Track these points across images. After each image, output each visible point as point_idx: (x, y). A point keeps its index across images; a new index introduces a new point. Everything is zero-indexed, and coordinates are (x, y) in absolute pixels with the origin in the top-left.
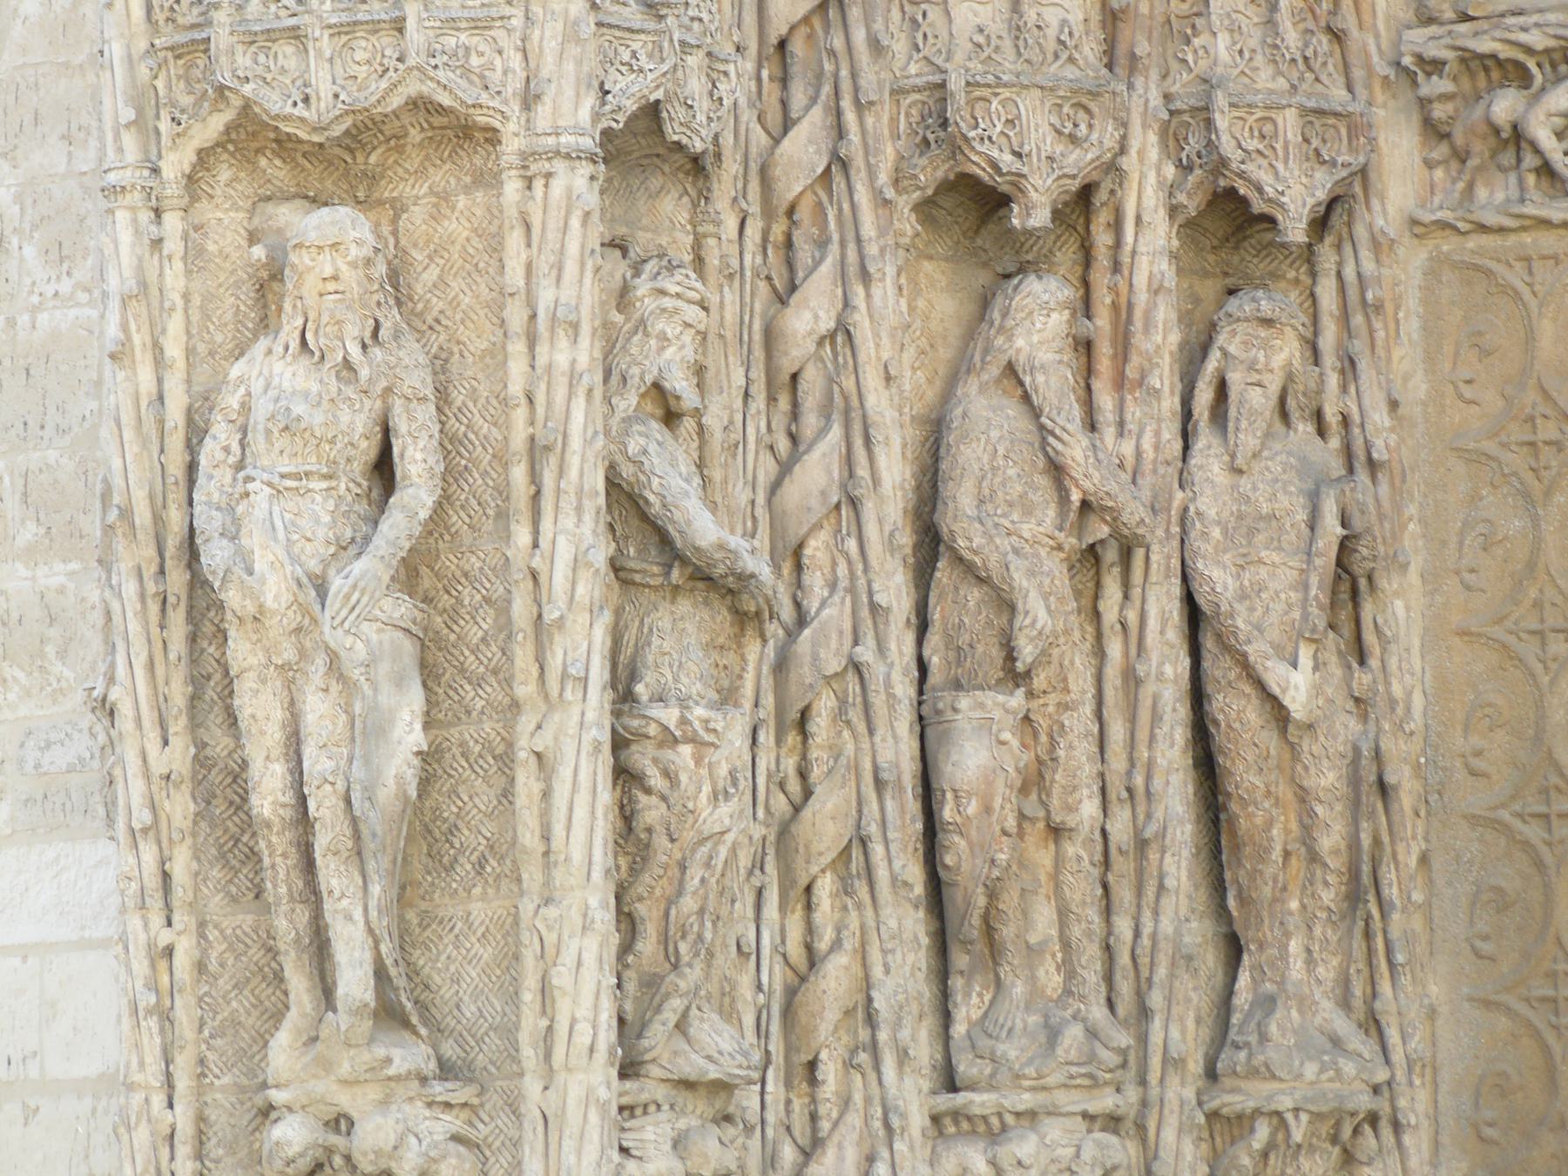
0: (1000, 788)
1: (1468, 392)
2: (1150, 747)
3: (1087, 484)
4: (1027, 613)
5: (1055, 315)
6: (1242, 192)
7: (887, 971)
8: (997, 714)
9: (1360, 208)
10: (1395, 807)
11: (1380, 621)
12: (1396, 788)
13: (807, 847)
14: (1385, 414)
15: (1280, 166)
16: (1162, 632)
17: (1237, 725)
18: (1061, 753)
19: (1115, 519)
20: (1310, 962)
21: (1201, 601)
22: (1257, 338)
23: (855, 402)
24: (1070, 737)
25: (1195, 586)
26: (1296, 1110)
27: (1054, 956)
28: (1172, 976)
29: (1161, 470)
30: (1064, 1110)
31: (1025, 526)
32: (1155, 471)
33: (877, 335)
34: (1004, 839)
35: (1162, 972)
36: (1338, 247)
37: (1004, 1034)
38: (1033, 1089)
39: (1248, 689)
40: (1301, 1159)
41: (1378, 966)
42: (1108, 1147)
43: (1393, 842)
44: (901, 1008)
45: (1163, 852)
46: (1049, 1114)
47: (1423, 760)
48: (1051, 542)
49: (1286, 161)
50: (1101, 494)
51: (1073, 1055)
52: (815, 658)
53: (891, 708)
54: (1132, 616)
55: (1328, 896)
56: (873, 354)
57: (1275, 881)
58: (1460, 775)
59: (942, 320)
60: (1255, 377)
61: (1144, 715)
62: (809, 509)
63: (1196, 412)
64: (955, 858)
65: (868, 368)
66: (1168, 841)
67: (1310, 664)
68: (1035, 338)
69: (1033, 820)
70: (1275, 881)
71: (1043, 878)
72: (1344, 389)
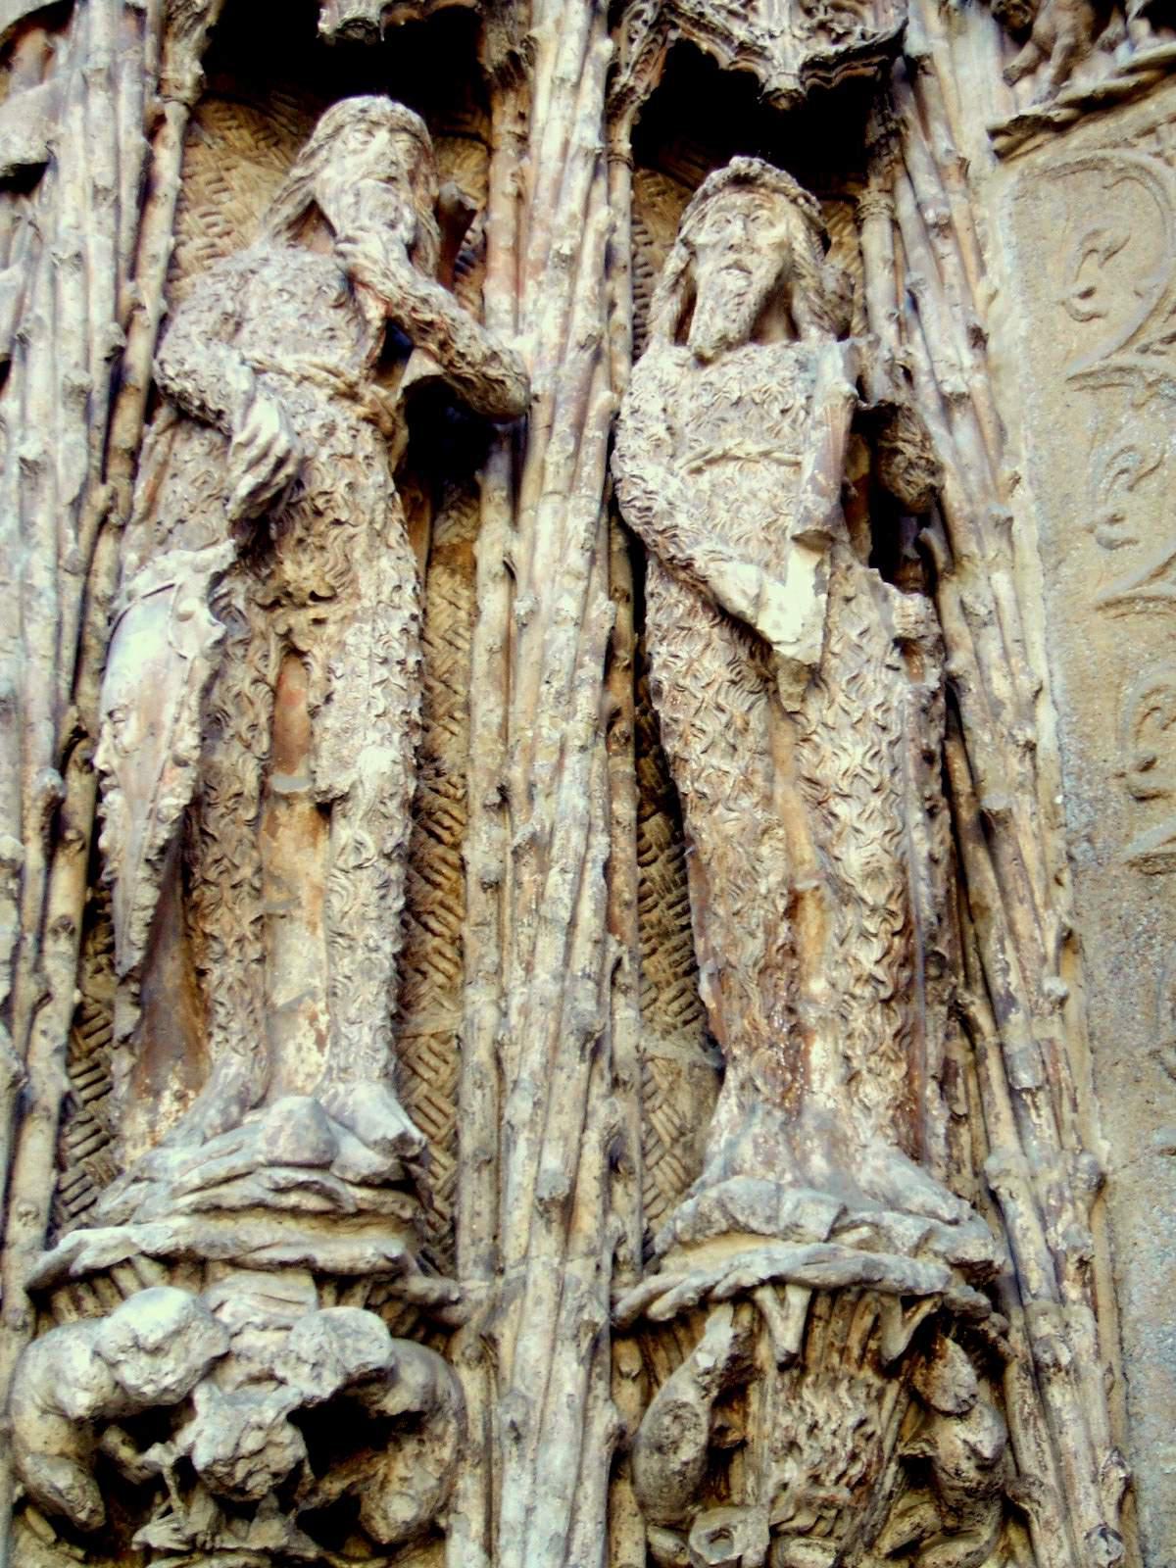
1: (1086, 306)
5: (382, 136)
6: (705, 46)
9: (914, 135)
10: (1006, 851)
11: (969, 599)
12: (1004, 819)
17: (687, 682)
19: (443, 345)
20: (851, 1078)
26: (778, 1282)
28: (550, 1066)
29: (571, 355)
30: (265, 1256)
32: (561, 359)
33: (90, 151)
36: (890, 192)
38: (197, 1211)
39: (703, 624)
40: (807, 1394)
41: (992, 1104)
42: (357, 1333)
45: (544, 869)
46: (234, 1264)
47: (1059, 799)
48: (333, 379)
49: (770, 16)
50: (411, 302)
51: (284, 1150)
54: (519, 549)
55: (868, 956)
58: (1120, 801)
60: (731, 257)
65: (69, 187)
66: (555, 851)
69: (288, 799)
70: (770, 931)
71: (305, 894)
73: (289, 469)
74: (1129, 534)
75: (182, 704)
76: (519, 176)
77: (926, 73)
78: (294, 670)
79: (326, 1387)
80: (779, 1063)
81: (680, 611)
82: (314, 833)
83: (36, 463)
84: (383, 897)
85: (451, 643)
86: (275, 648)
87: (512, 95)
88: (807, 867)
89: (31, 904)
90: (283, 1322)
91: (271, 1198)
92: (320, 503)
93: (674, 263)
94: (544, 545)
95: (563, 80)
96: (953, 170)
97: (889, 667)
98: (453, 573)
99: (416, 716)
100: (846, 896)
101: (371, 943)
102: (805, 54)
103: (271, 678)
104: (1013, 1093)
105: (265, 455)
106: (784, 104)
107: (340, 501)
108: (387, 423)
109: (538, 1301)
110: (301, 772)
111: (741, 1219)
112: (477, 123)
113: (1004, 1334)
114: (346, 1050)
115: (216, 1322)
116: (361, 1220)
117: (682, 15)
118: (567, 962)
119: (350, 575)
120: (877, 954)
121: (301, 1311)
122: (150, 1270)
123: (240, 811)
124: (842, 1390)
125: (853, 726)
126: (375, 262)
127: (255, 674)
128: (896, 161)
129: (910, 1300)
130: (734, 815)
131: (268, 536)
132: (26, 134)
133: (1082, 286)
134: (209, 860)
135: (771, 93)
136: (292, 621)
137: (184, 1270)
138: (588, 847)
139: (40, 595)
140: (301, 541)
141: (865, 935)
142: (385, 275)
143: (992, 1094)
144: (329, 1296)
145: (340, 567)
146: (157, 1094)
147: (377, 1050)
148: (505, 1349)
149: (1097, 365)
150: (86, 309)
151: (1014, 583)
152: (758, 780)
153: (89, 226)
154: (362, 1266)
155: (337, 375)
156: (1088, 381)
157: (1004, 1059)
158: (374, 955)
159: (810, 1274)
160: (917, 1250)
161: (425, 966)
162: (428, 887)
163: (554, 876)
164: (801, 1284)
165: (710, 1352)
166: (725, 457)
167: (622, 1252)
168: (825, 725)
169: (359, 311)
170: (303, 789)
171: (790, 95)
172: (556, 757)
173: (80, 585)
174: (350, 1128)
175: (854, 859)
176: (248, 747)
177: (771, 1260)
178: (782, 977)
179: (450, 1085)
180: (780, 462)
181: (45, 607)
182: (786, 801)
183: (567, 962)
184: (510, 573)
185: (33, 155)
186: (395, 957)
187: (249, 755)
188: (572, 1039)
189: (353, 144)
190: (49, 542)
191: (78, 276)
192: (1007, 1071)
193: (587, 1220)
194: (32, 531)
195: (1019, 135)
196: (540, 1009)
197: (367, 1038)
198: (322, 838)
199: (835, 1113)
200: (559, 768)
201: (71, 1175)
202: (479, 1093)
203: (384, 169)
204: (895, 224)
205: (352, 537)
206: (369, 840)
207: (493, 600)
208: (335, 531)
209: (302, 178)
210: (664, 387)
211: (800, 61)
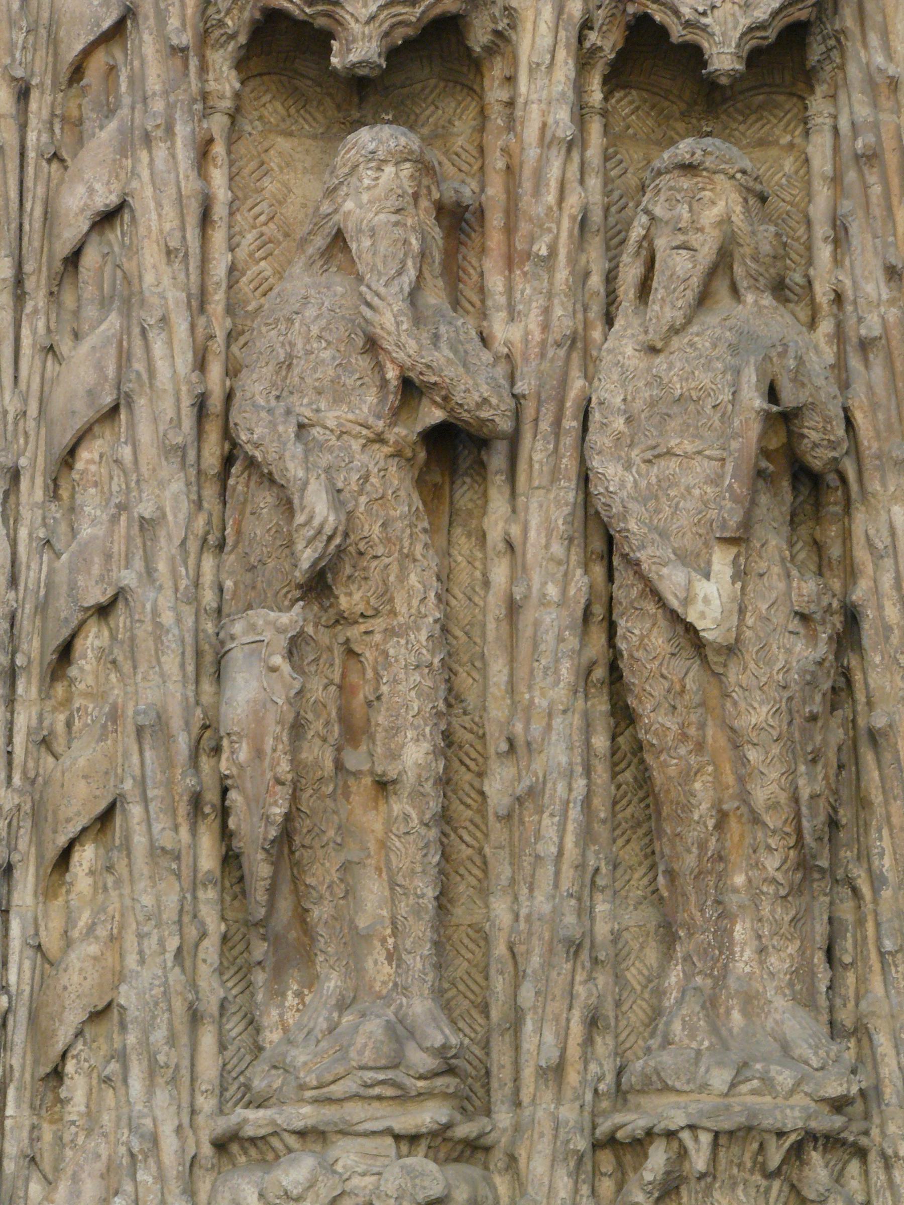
2: (530, 688)
3: (400, 356)
4: (303, 509)
5: (389, 169)
6: (658, 18)
7: (142, 962)
8: (267, 636)
9: (853, 46)
10: (888, 756)
11: (872, 532)
13: (55, 813)
14: (882, 285)
17: (640, 654)
18: (385, 689)
19: (446, 399)
20: (762, 951)
22: (679, 191)
24: (394, 669)
27: (384, 941)
29: (550, 354)
30: (361, 1128)
31: (331, 414)
32: (543, 355)
33: (159, 205)
34: (278, 788)
35: (536, 960)
37: (301, 1037)
38: (316, 1101)
40: (717, 1194)
43: (886, 803)
44: (156, 1004)
45: (540, 811)
46: (343, 1133)
48: (365, 432)
51: (368, 1057)
52: (73, 586)
53: (158, 640)
54: (515, 531)
55: (772, 863)
56: (154, 225)
57: (702, 846)
59: (304, 206)
60: (681, 238)
61: (524, 647)
62: (73, 413)
63: (621, 292)
67: (729, 571)
68: (365, 197)
69: (357, 774)
70: (702, 846)
71: (372, 846)
72: (837, 261)
73: (337, 541)
75: (277, 739)
78: (352, 663)
80: (709, 944)
81: (634, 593)
82: (376, 800)
83: (152, 519)
84: (425, 855)
85: (470, 599)
86: (338, 651)
87: (499, 59)
88: (731, 791)
89: (186, 872)
90: (375, 1170)
91: (362, 1091)
92: (362, 546)
93: (636, 232)
94: (532, 534)
95: (538, 64)
96: (884, 90)
97: (791, 632)
98: (469, 536)
99: (442, 706)
100: (756, 820)
103: (337, 680)
104: (882, 954)
105: (319, 532)
106: (724, 81)
107: (377, 540)
108: (408, 453)
109: (542, 1135)
110: (363, 748)
111: (670, 1083)
112: (471, 76)
113: (866, 1133)
114: (407, 972)
115: (334, 1172)
116: (422, 1098)
118: (556, 886)
119: (389, 594)
120: (777, 864)
121: (386, 1161)
122: (292, 1141)
123: (324, 788)
124: (740, 1192)
125: (760, 689)
126: (389, 334)
127: (326, 681)
128: (837, 67)
130: (675, 761)
131: (326, 582)
132: (106, 178)
134: (305, 831)
135: (710, 73)
136: (349, 634)
137: (310, 1138)
138: (570, 790)
139: (168, 632)
140: (349, 577)
142: (399, 346)
143: (868, 950)
144: (404, 1148)
146: (283, 995)
147: (426, 974)
150: (173, 365)
152: (692, 731)
153: (166, 281)
154: (424, 1130)
155: (368, 427)
157: (878, 925)
158: (421, 901)
160: (792, 1092)
161: (462, 871)
162: (462, 807)
163: (546, 821)
165: (652, 1170)
167: (602, 1087)
168: (741, 687)
169: (379, 367)
170: (366, 767)
171: (727, 73)
172: (546, 719)
173: (194, 610)
174: (412, 1034)
175: (760, 795)
176: (325, 740)
177: (688, 1115)
178: (711, 881)
179: (483, 964)
180: (710, 458)
181: (171, 641)
182: (715, 741)
183: (556, 886)
185: (113, 199)
186: (437, 898)
187: (326, 746)
188: (560, 945)
189: (367, 182)
190: (168, 584)
191: (163, 335)
192: (879, 939)
193: (573, 1077)
194: (156, 575)
196: (538, 923)
197: (419, 965)
198: (381, 802)
199: (751, 975)
200: (549, 727)
201: (232, 1049)
202: (500, 978)
204: (836, 131)
205: (387, 566)
206: (414, 816)
207: (500, 573)
208: (374, 564)
209: (329, 214)
211: (741, 29)
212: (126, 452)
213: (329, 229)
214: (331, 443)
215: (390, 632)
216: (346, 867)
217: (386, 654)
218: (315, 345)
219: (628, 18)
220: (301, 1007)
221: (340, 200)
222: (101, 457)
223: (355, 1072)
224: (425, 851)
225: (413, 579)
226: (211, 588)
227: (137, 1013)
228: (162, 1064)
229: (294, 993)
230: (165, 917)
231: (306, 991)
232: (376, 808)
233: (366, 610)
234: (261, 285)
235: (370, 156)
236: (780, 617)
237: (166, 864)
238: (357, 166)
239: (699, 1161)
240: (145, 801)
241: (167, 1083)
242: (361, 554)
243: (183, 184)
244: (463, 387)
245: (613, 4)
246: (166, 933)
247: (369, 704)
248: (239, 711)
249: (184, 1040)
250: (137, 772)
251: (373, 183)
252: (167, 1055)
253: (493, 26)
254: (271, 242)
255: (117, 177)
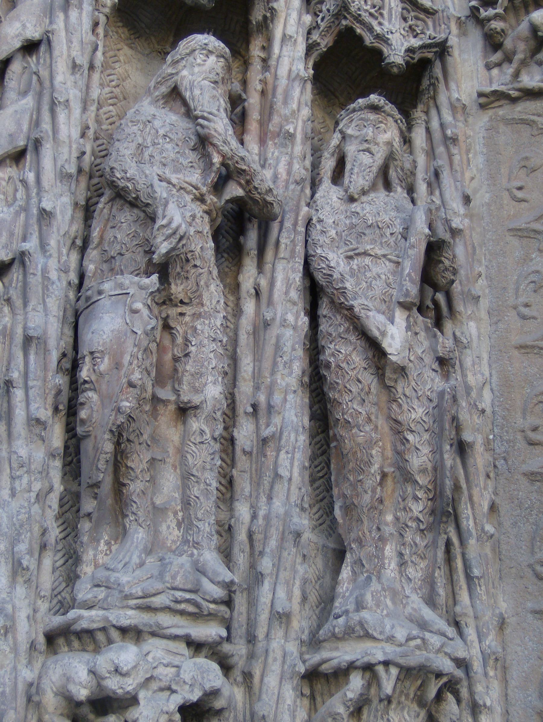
0: (130, 348)
1: (520, 194)
2: (273, 373)
3: (225, 149)
6: (359, 31)
7: (13, 494)
8: (131, 291)
9: (442, 86)
10: (470, 461)
11: (458, 334)
12: (471, 445)
15: (386, 23)
16: (287, 293)
17: (344, 365)
18: (193, 349)
20: (402, 564)
21: (319, 277)
22: (367, 120)
23: (47, 84)
25: (315, 264)
26: (386, 664)
28: (281, 547)
29: (292, 187)
32: (287, 187)
35: (273, 543)
36: (427, 113)
37: (120, 566)
38: (139, 608)
39: (353, 338)
40: (391, 713)
44: (21, 526)
45: (278, 450)
46: (154, 634)
47: (491, 437)
48: (194, 191)
49: (390, 21)
50: (236, 158)
51: (179, 582)
53: (45, 288)
54: (263, 283)
55: (417, 508)
56: (65, 53)
58: (521, 444)
60: (366, 146)
61: (269, 350)
64: (89, 412)
65: (59, 59)
66: (283, 442)
67: (404, 324)
69: (165, 402)
70: (374, 491)
71: (171, 450)
74: (535, 314)
76: (264, 82)
77: (449, 55)
79: (195, 696)
80: (373, 554)
81: (342, 329)
84: (213, 459)
88: (389, 461)
91: (172, 605)
96: (459, 110)
97: (433, 370)
101: (208, 482)
102: (406, 45)
104: (469, 578)
105: (174, 233)
106: (395, 70)
109: (275, 660)
111: (370, 631)
117: (349, 13)
118: (288, 498)
119: (198, 293)
120: (421, 508)
122: (115, 634)
125: (418, 398)
126: (220, 134)
128: (431, 98)
129: (439, 675)
130: (363, 434)
132: (34, 23)
133: (519, 184)
134: (131, 430)
135: (389, 63)
136: (169, 312)
137: (132, 634)
138: (296, 441)
139: (53, 283)
140: (179, 273)
141: (416, 499)
142: (225, 143)
143: (458, 576)
145: (194, 288)
146: (98, 541)
147: (212, 535)
148: (256, 679)
149: (524, 226)
151: (478, 328)
152: (373, 418)
153: (69, 84)
155: (197, 188)
156: (517, 232)
158: (209, 488)
159: (401, 661)
160: (439, 651)
164: (397, 665)
165: (352, 691)
166: (365, 254)
168: (405, 395)
171: (398, 66)
172: (284, 394)
174: (204, 573)
177: (385, 653)
180: (390, 260)
182: (382, 428)
183: (288, 498)
184: (257, 294)
188: (291, 536)
189: (199, 61)
191: (66, 111)
194: (47, 248)
195: (492, 99)
196: (276, 519)
200: (285, 400)
202: (242, 554)
203: (213, 76)
205: (200, 274)
206: (207, 431)
208: (193, 271)
209: (173, 74)
210: (334, 211)
212: (31, 177)
213: (171, 83)
214: (173, 192)
215: (197, 316)
216: (153, 461)
217: (195, 329)
218: (161, 141)
219: (342, 27)
220: (108, 552)
221: (180, 68)
222: (9, 179)
223: (168, 591)
224: (212, 457)
225: (213, 288)
226: (74, 272)
227: (7, 530)
228: (25, 566)
229: (105, 542)
230: (33, 467)
231: (113, 542)
232: (176, 426)
233: (185, 298)
234: (109, 118)
235: (204, 46)
236: (428, 359)
237: (38, 431)
238: (195, 50)
239: (388, 687)
240: (27, 389)
241: (25, 582)
242: (188, 260)
243: (84, 36)
244: (260, 178)
245: (332, 20)
246: (33, 478)
247: (176, 359)
248: (105, 337)
249: (36, 555)
250: (22, 368)
251: (202, 63)
252: (29, 561)
253: (265, 13)
254: (116, 98)
255: (40, 25)
